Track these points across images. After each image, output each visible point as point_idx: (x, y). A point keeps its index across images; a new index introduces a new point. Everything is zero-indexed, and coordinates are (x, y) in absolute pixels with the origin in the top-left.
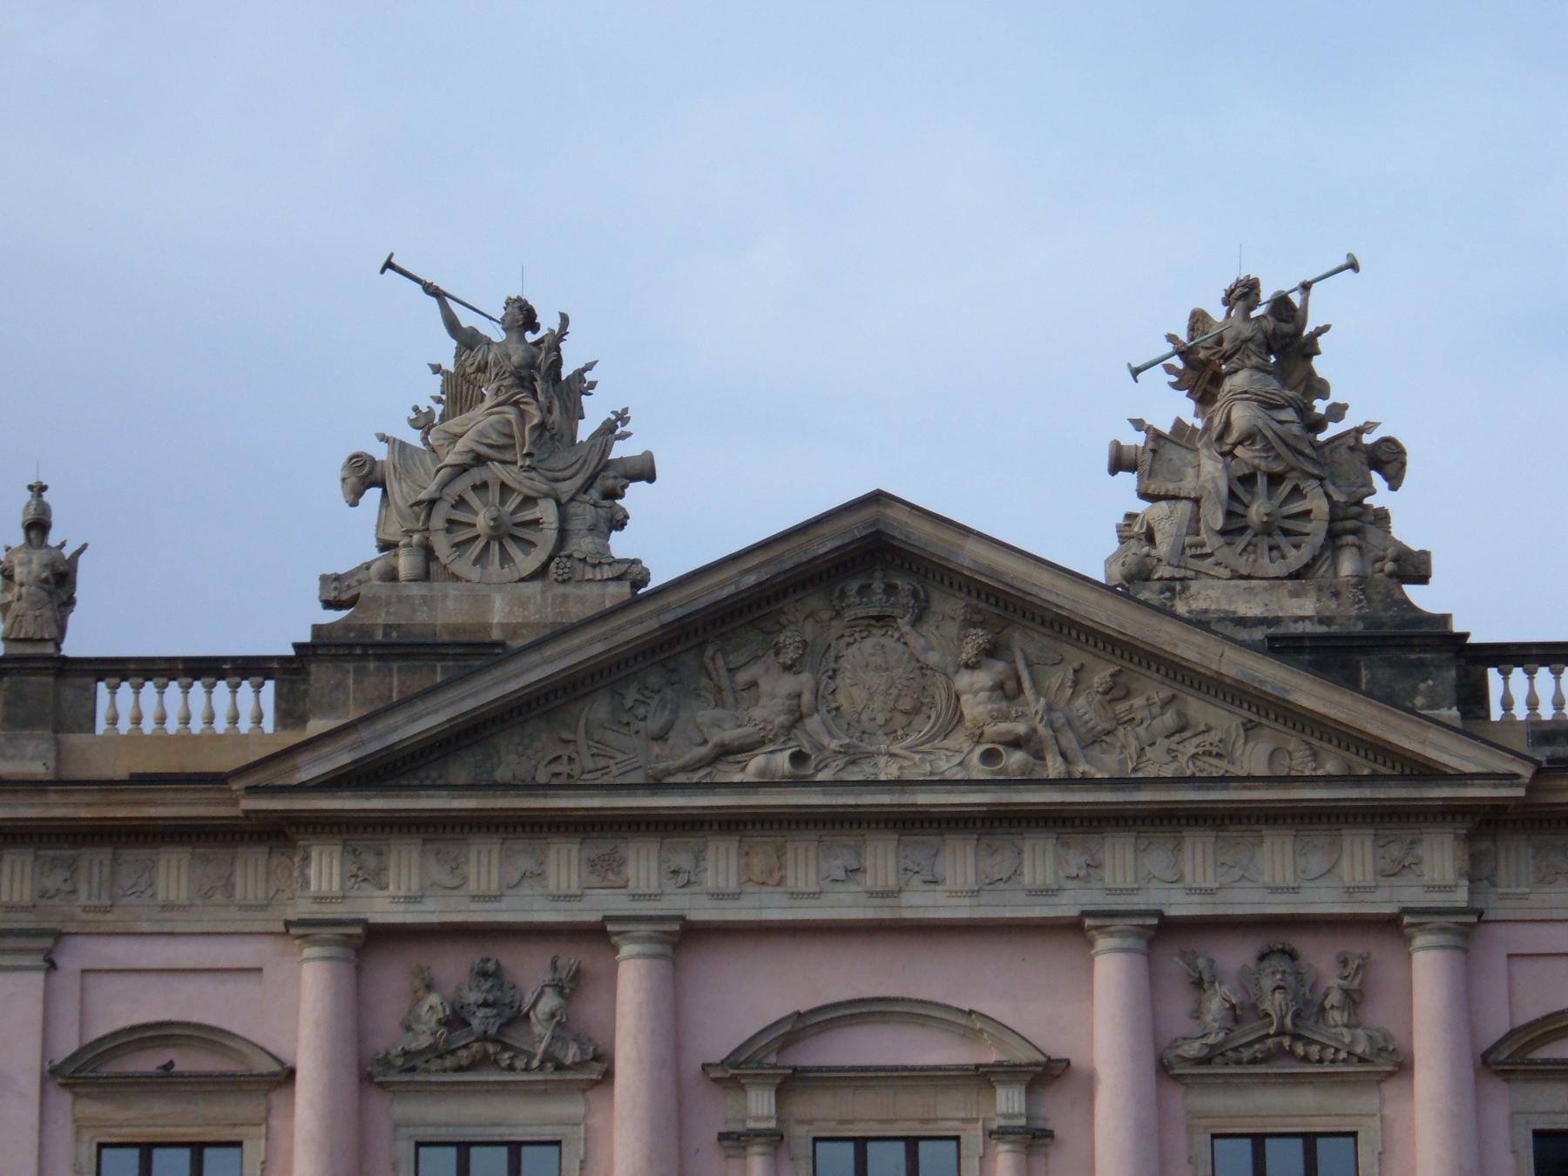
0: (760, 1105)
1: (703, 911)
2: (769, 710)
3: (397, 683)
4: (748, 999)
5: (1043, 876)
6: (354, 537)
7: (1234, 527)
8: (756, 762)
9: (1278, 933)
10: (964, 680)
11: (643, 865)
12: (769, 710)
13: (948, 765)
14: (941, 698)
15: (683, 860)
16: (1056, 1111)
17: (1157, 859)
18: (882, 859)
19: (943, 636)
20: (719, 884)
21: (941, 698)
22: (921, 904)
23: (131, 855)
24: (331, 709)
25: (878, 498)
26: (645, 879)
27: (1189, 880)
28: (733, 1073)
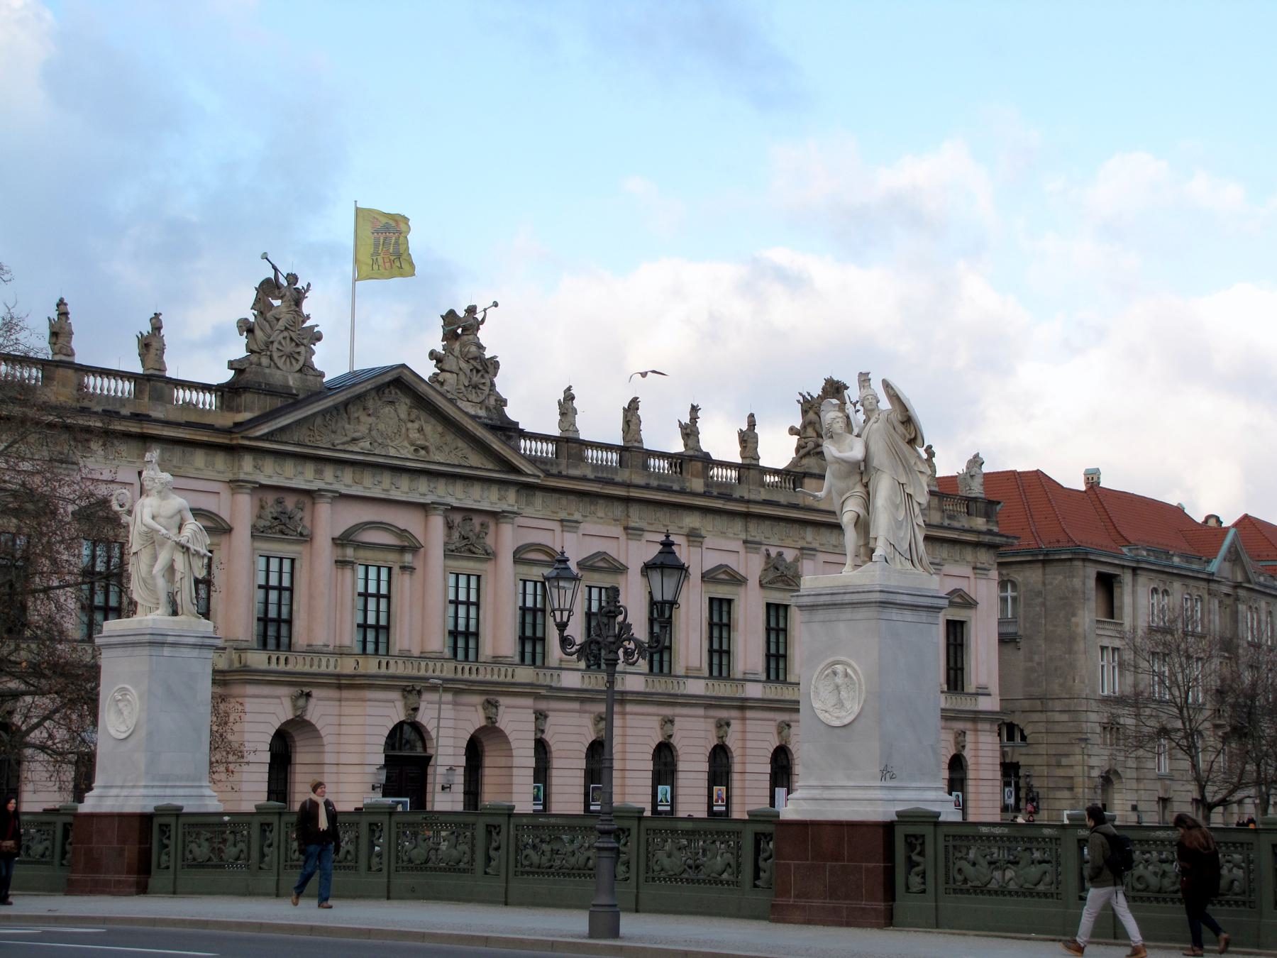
1: (344, 491)
2: (363, 429)
5: (422, 491)
6: (238, 349)
8: (362, 444)
9: (468, 512)
10: (410, 425)
11: (329, 472)
12: (363, 429)
13: (401, 451)
14: (404, 430)
15: (339, 473)
17: (450, 489)
18: (386, 479)
20: (346, 482)
21: (404, 430)
22: (396, 495)
23: (188, 450)
24: (251, 410)
25: (404, 366)
26: (329, 479)
27: (457, 496)
28: (342, 541)
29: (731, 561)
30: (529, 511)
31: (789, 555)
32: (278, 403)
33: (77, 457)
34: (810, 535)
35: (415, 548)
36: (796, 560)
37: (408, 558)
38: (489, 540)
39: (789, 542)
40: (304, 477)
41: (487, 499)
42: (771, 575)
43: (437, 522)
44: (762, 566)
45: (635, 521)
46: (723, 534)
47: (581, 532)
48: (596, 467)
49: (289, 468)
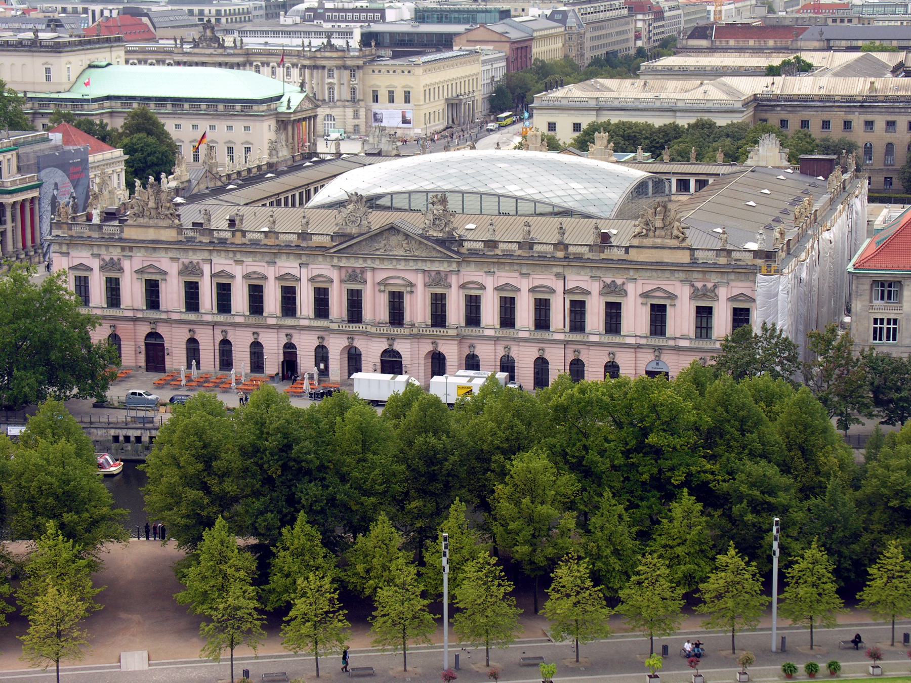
0: (382, 288)
2: (382, 245)
3: (342, 239)
4: (381, 276)
5: (412, 265)
7: (434, 224)
9: (438, 272)
12: (382, 245)
16: (414, 289)
18: (394, 262)
19: (400, 237)
20: (377, 264)
22: (398, 267)
26: (369, 263)
27: (428, 266)
28: (379, 284)
29: (584, 286)
30: (468, 269)
31: (619, 282)
32: (342, 239)
33: (277, 260)
34: (632, 273)
35: (412, 285)
36: (623, 284)
37: (409, 289)
38: (449, 280)
39: (619, 276)
40: (359, 264)
41: (443, 267)
42: (605, 291)
43: (420, 276)
44: (602, 286)
45: (524, 271)
46: (579, 274)
47: (496, 276)
48: (503, 251)
49: (352, 261)
